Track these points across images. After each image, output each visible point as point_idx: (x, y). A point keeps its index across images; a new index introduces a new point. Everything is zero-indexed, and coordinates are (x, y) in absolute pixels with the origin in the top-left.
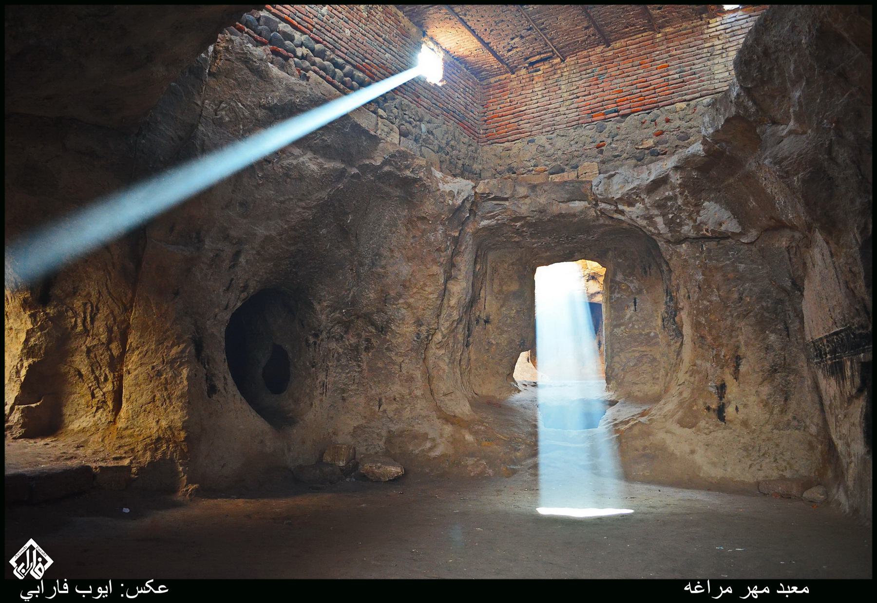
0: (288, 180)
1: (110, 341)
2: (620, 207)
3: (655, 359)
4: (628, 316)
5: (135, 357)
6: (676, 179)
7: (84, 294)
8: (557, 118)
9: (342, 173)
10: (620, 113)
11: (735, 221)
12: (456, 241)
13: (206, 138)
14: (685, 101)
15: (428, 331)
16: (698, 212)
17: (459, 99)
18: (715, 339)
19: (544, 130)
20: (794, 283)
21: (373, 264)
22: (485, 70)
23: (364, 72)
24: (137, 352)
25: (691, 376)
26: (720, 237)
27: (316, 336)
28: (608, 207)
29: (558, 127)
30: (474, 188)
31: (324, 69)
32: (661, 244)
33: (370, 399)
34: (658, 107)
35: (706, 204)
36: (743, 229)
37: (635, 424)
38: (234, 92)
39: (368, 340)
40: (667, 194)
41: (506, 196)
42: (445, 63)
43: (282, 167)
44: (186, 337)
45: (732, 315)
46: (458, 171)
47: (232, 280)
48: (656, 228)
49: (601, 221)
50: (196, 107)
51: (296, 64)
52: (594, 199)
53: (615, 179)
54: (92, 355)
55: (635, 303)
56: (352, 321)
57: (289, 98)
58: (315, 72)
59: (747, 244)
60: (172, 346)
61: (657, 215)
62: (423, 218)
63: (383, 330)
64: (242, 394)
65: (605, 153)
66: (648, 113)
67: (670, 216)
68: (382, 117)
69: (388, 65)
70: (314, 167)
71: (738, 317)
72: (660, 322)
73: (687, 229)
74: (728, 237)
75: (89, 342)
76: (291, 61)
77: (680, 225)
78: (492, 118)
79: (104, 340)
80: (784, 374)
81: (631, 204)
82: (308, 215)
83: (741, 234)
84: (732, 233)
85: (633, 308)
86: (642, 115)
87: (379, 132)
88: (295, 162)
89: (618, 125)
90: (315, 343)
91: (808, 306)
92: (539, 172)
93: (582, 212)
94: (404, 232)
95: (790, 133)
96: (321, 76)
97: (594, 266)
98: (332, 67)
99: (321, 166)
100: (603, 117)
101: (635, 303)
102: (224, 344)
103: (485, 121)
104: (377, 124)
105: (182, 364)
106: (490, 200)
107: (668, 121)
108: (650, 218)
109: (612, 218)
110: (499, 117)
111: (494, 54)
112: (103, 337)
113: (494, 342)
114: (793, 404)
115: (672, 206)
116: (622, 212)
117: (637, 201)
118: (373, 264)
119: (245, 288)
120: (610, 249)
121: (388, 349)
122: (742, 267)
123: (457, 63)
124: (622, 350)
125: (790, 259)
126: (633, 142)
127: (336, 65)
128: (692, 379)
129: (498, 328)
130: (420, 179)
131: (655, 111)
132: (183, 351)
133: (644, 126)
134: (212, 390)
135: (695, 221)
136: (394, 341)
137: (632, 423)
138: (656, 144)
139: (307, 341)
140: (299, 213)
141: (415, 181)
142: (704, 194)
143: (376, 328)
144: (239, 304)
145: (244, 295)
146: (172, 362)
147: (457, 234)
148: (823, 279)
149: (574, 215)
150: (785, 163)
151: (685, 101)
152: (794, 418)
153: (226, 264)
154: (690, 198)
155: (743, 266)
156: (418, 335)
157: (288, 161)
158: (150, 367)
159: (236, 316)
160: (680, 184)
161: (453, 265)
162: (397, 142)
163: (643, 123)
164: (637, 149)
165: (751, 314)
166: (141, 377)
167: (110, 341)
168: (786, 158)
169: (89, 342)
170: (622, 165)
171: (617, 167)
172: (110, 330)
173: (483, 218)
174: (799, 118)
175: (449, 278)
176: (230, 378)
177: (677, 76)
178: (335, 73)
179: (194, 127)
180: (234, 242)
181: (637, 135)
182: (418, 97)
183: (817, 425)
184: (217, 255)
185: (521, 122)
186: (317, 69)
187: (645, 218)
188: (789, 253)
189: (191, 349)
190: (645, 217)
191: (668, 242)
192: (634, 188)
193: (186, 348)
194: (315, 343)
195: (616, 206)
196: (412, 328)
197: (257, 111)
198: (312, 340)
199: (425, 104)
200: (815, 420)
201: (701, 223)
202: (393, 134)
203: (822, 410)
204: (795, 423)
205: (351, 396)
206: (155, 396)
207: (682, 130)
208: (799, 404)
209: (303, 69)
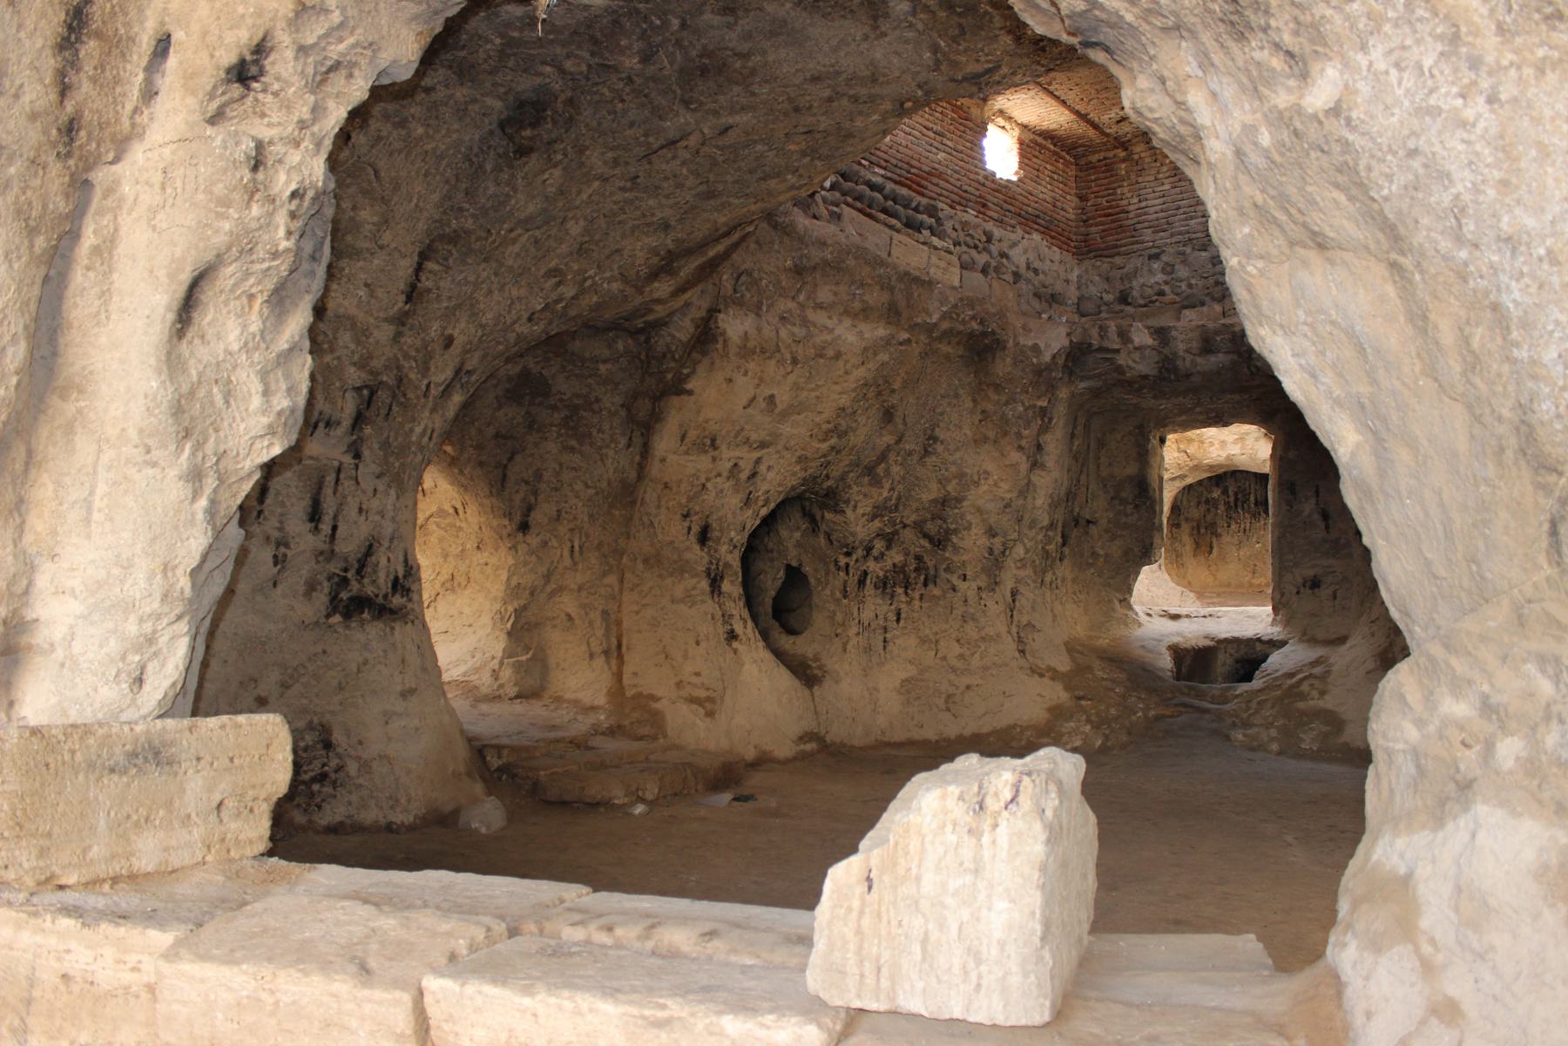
4: (1306, 513)
9: (888, 342)
15: (1004, 544)
17: (1044, 192)
22: (1082, 145)
23: (910, 188)
31: (859, 198)
42: (1021, 142)
51: (825, 200)
56: (896, 533)
58: (848, 205)
68: (936, 248)
69: (942, 169)
82: (844, 401)
85: (1313, 501)
88: (829, 338)
90: (847, 565)
94: (969, 404)
111: (1095, 126)
113: (1101, 552)
121: (947, 570)
123: (1040, 140)
127: (873, 187)
129: (1107, 531)
134: (732, 636)
136: (955, 558)
137: (1300, 676)
139: (836, 562)
141: (984, 334)
143: (931, 540)
147: (1045, 404)
161: (1039, 447)
162: (957, 283)
173: (1082, 379)
175: (1035, 465)
182: (984, 206)
186: (849, 199)
194: (847, 565)
196: (983, 541)
198: (843, 561)
199: (995, 215)
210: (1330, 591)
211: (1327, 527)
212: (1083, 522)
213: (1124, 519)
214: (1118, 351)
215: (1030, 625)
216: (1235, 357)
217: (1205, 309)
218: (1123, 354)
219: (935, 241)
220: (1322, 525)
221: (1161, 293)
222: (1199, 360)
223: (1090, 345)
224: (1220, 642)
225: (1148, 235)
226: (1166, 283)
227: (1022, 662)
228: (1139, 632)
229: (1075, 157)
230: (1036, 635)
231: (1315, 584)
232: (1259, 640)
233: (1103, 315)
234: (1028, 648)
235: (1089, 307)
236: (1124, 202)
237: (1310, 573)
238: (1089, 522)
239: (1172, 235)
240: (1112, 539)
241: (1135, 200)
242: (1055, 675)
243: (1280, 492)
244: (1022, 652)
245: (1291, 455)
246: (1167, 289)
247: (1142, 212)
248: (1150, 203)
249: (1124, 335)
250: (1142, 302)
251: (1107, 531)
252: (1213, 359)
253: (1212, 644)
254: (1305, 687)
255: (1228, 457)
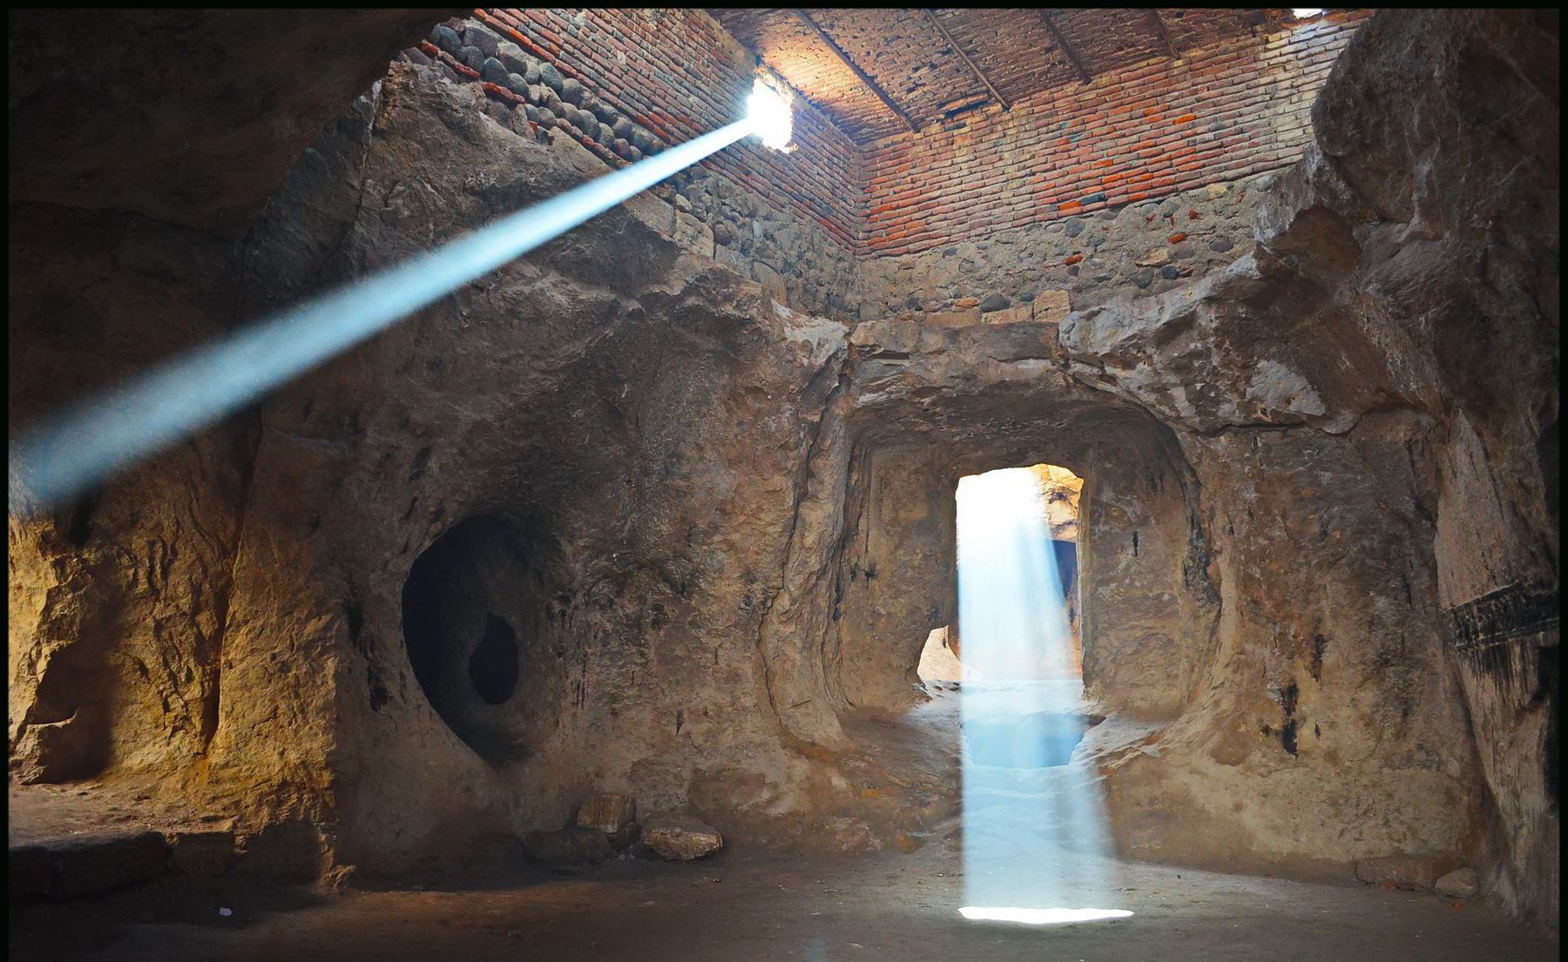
0: (516, 322)
1: (196, 609)
2: (1109, 370)
3: (1170, 642)
4: (1122, 565)
5: (241, 639)
6: (1208, 319)
7: (150, 525)
8: (996, 211)
9: (611, 310)
10: (1109, 201)
11: (1314, 396)
12: (816, 431)
13: (368, 247)
14: (1225, 180)
15: (765, 592)
16: (1248, 380)
17: (821, 177)
18: (1278, 606)
19: (973, 233)
20: (1419, 506)
21: (667, 471)
22: (868, 125)
23: (650, 129)
24: (244, 630)
25: (1235, 672)
26: (1287, 423)
27: (565, 600)
28: (1087, 370)
29: (998, 227)
30: (847, 335)
31: (580, 123)
32: (1182, 436)
33: (661, 714)
34: (1177, 192)
35: (1262, 364)
36: (1328, 409)
37: (1136, 758)
38: (418, 164)
39: (658, 608)
40: (1192, 346)
41: (904, 351)
42: (796, 112)
43: (504, 299)
44: (333, 602)
45: (1308, 564)
46: (819, 306)
47: (415, 500)
48: (1173, 408)
49: (1075, 395)
50: (351, 191)
51: (530, 115)
52: (1062, 356)
53: (1100, 320)
54: (165, 634)
57: (518, 175)
58: (563, 128)
59: (1336, 435)
60: (308, 619)
61: (1175, 385)
62: (756, 391)
63: (684, 589)
64: (433, 704)
65: (1082, 274)
66: (1159, 202)
67: (1199, 386)
68: (682, 209)
69: (694, 116)
70: (560, 298)
71: (1320, 566)
72: (1179, 576)
73: (1228, 410)
74: (1301, 424)
75: (160, 611)
76: (520, 110)
77: (1217, 402)
78: (880, 211)
79: (186, 608)
80: (1401, 669)
81: (1128, 365)
82: (550, 383)
83: (1325, 418)
84: (1309, 416)
85: (1131, 551)
86: (1148, 205)
87: (677, 236)
88: (527, 290)
89: (1106, 224)
90: (563, 613)
91: (1445, 547)
92: (964, 308)
93: (1040, 379)
94: (723, 414)
96: (574, 136)
97: (1062, 475)
98: (594, 120)
99: (574, 297)
100: (1078, 209)
102: (400, 615)
103: (868, 216)
104: (675, 221)
105: (325, 651)
106: (876, 357)
107: (1194, 216)
108: (1162, 390)
109: (1094, 389)
111: (884, 96)
112: (185, 603)
113: (883, 612)
114: (1417, 723)
115: (1201, 368)
116: (1112, 380)
117: (1138, 360)
118: (667, 471)
119: (439, 514)
120: (1090, 445)
121: (693, 624)
122: (1326, 476)
123: (817, 112)
124: (1112, 626)
125: (1413, 463)
126: (1131, 254)
127: (601, 116)
128: (1238, 678)
129: (889, 586)
130: (752, 320)
131: (1172, 198)
132: (327, 628)
133: (1152, 225)
134: (380, 696)
135: (1243, 395)
136: (704, 609)
137: (1130, 756)
138: (1174, 257)
139: (549, 609)
140: (534, 381)
141: (743, 323)
142: (1258, 348)
144: (428, 543)
145: (436, 528)
146: (307, 648)
147: (817, 419)
148: (1472, 499)
149: (1026, 385)
151: (1225, 180)
152: (1420, 747)
153: (404, 472)
154: (1233, 355)
155: (1328, 475)
156: (748, 599)
157: (516, 288)
158: (268, 656)
159: (419, 566)
160: (1216, 329)
161: (809, 474)
162: (709, 254)
163: (1150, 220)
164: (1140, 266)
165: (1344, 561)
166: (251, 674)
167: (196, 609)
169: (160, 611)
170: (1111, 296)
171: (1103, 299)
172: (196, 590)
173: (864, 389)
175: (802, 496)
176: (410, 676)
177: (1210, 136)
178: (599, 131)
179: (346, 227)
180: (419, 432)
181: (1139, 242)
182: (748, 174)
183: (1461, 759)
184: (388, 456)
185: (931, 219)
186: (567, 123)
187: (1154, 390)
188: (1411, 452)
189: (342, 624)
191: (1194, 432)
192: (1133, 336)
193: (332, 621)
194: (563, 613)
195: (1102, 368)
196: (737, 587)
197: (460, 199)
198: (557, 607)
199: (759, 186)
200: (1458, 751)
201: (1253, 398)
202: (703, 239)
203: (1470, 733)
204: (1422, 756)
205: (628, 708)
206: (277, 708)
207: (1220, 232)
208: (1428, 721)
209: (541, 123)
219: (681, 200)
229: (861, 142)
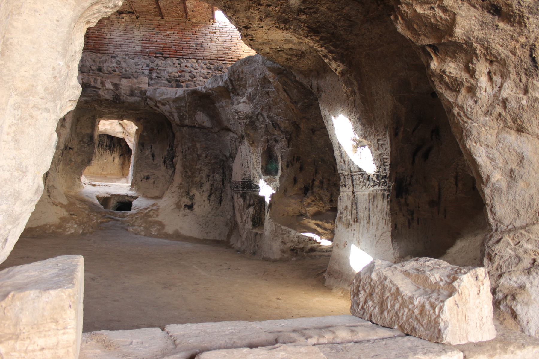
2: (158, 105)
3: (158, 177)
4: (147, 154)
10: (164, 55)
18: (192, 174)
26: (202, 127)
35: (199, 112)
48: (173, 118)
55: (151, 148)
67: (181, 114)
73: (187, 122)
77: (185, 119)
81: (163, 104)
83: (212, 128)
85: (150, 150)
89: (162, 61)
95: (244, 102)
101: (151, 148)
107: (186, 66)
110: (96, 37)
113: (73, 160)
116: (158, 107)
124: (142, 171)
128: (179, 191)
129: (76, 152)
137: (149, 209)
150: (240, 114)
151: (196, 59)
168: (240, 112)
174: (248, 98)
177: (194, 45)
190: (169, 112)
191: (177, 125)
200: (230, 213)
203: (234, 209)
208: (224, 206)
210: (152, 181)
211: (153, 160)
212: (68, 148)
213: (83, 149)
214: (100, 89)
215: (53, 186)
216: (141, 99)
217: (130, 80)
218: (101, 90)
220: (151, 158)
221: (115, 71)
222: (128, 98)
223: (90, 84)
224: (112, 195)
225: (112, 49)
226: (117, 67)
227: (49, 200)
228: (84, 190)
230: (55, 190)
231: (148, 178)
232: (127, 196)
233: (91, 74)
234: (51, 195)
235: (85, 69)
236: (105, 34)
237: (146, 174)
238: (70, 148)
239: (121, 51)
240: (79, 155)
241: (109, 35)
242: (62, 206)
243: (139, 146)
244: (49, 196)
245: (144, 134)
246: (117, 70)
247: (111, 40)
248: (114, 37)
249: (103, 83)
250: (107, 72)
251: (76, 152)
252: (133, 98)
253: (109, 196)
254: (151, 213)
255: (105, 130)
